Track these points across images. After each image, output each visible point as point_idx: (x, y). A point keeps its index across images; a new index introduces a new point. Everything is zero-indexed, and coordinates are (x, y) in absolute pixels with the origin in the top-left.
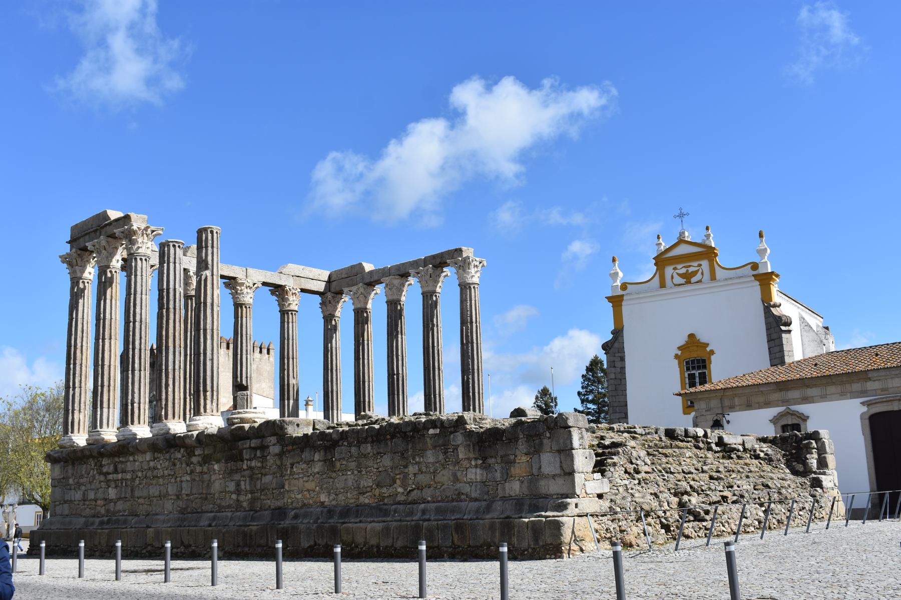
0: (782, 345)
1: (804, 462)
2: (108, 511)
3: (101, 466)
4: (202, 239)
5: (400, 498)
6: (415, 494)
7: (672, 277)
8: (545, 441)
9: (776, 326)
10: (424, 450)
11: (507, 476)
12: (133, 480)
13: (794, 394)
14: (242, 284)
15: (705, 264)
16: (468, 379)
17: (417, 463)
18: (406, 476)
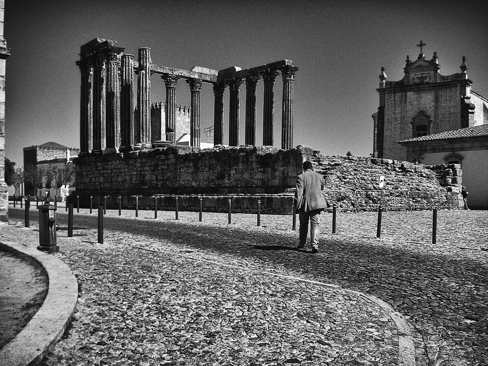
0: (468, 120)
1: (445, 181)
2: (101, 187)
3: (98, 166)
4: (141, 57)
5: (228, 185)
6: (234, 183)
7: (414, 79)
8: (291, 160)
9: (466, 109)
10: (238, 163)
11: (274, 177)
12: (111, 173)
13: (457, 146)
14: (170, 77)
15: (432, 72)
16: (285, 130)
17: (235, 169)
18: (230, 175)
